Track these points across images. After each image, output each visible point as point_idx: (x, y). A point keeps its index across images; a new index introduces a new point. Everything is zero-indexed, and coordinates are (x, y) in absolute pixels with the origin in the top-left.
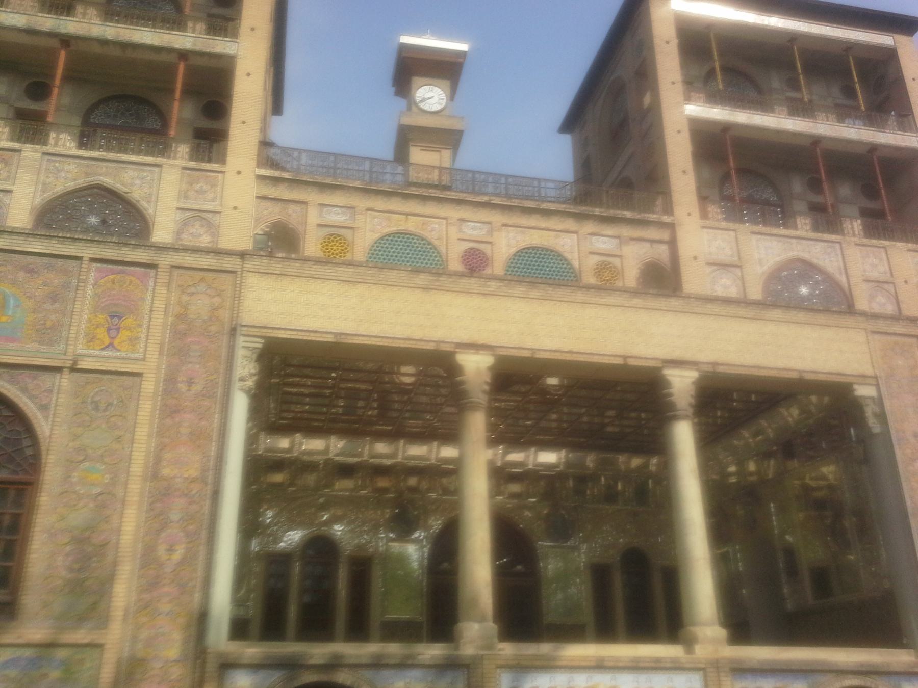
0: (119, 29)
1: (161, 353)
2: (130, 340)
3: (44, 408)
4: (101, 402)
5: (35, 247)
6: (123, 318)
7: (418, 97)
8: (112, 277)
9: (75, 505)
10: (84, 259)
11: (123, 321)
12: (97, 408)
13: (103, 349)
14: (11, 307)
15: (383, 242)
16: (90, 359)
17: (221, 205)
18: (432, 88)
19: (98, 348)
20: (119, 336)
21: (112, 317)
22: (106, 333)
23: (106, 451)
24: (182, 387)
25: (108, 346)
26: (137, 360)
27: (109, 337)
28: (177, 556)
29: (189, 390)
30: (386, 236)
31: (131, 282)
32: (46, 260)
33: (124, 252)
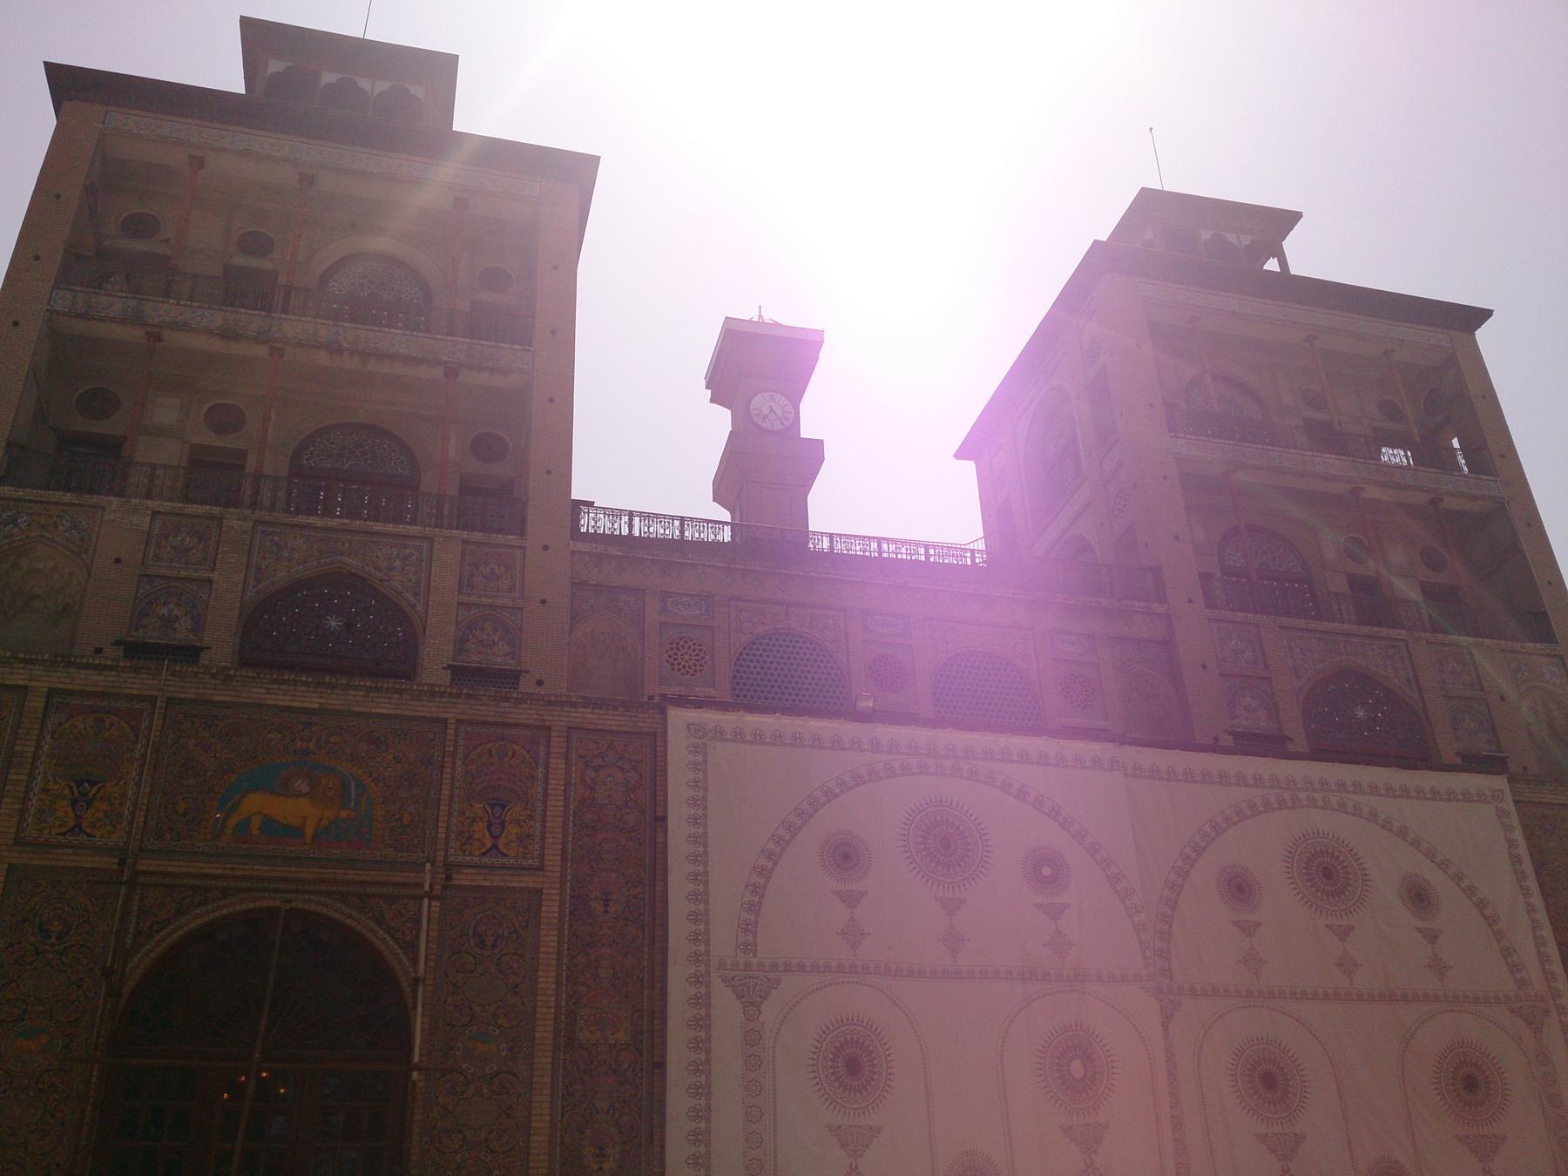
1: (564, 858)
4: (486, 935)
5: (381, 705)
7: (753, 409)
8: (488, 746)
10: (450, 721)
11: (509, 810)
13: (484, 854)
14: (353, 796)
15: (755, 647)
16: (469, 871)
17: (523, 598)
18: (773, 396)
19: (477, 853)
20: (504, 835)
21: (493, 806)
22: (486, 830)
23: (498, 1008)
24: (598, 907)
25: (490, 850)
26: (530, 868)
27: (491, 835)
28: (609, 1165)
29: (606, 911)
30: (757, 639)
31: (514, 752)
33: (503, 710)
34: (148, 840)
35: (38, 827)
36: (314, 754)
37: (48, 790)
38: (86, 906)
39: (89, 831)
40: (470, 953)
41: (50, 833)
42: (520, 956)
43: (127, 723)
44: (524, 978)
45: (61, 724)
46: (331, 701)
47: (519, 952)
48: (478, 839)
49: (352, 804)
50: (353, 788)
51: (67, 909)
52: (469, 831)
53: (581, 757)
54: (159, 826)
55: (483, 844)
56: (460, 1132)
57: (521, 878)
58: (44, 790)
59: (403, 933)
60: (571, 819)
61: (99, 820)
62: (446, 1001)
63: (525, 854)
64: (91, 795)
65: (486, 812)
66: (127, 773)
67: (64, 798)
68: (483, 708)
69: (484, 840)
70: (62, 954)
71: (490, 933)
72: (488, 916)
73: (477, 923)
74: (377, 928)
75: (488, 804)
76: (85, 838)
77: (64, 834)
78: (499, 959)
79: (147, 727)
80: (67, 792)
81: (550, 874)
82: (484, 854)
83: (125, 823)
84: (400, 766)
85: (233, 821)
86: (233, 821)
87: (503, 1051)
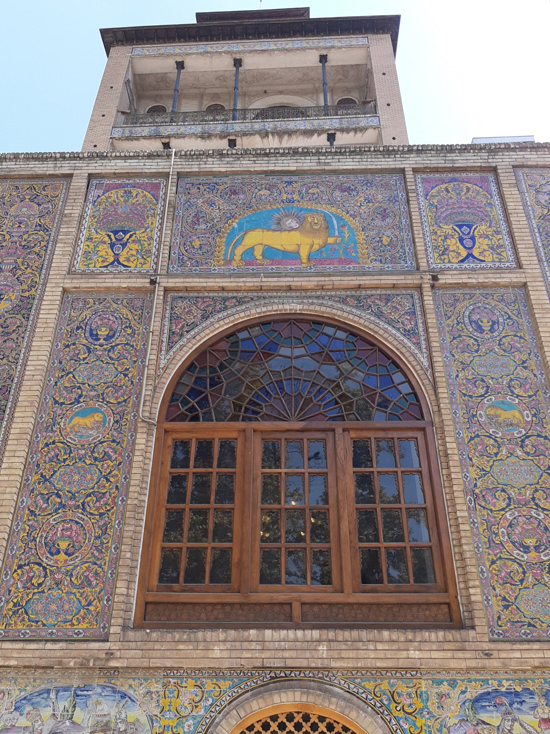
0: (276, 123)
2: (492, 248)
3: (410, 333)
4: (482, 322)
5: (346, 164)
6: (475, 227)
8: (444, 186)
9: (496, 454)
10: (406, 169)
11: (475, 229)
12: (480, 327)
13: (462, 261)
14: (336, 227)
21: (460, 227)
22: (458, 244)
23: (511, 380)
31: (468, 189)
32: (361, 177)
34: (173, 267)
35: (85, 263)
36: (299, 201)
37: (92, 239)
38: (127, 315)
39: (125, 263)
40: (471, 337)
41: (95, 266)
42: (521, 337)
43: (149, 193)
44: (530, 354)
45: (99, 196)
46: (304, 165)
47: (519, 335)
48: (453, 251)
49: (337, 234)
50: (335, 222)
51: (111, 318)
52: (444, 246)
53: (529, 186)
54: (181, 257)
55: (459, 254)
56: (503, 490)
57: (503, 275)
58: (89, 239)
59: (403, 323)
60: (536, 230)
61: (133, 255)
62: (457, 376)
63: (501, 259)
64: (125, 239)
65: (455, 230)
66: (152, 224)
67: (105, 243)
68: (431, 158)
69: (459, 251)
70: (109, 351)
71: (485, 320)
72: (479, 307)
73: (470, 313)
74: (378, 321)
75: (456, 226)
76: (123, 268)
77: (106, 266)
78: (500, 340)
79: (164, 194)
80: (107, 239)
81: (530, 271)
82: (462, 261)
83: (153, 257)
84: (371, 205)
85: (239, 251)
86: (239, 251)
87: (528, 417)
